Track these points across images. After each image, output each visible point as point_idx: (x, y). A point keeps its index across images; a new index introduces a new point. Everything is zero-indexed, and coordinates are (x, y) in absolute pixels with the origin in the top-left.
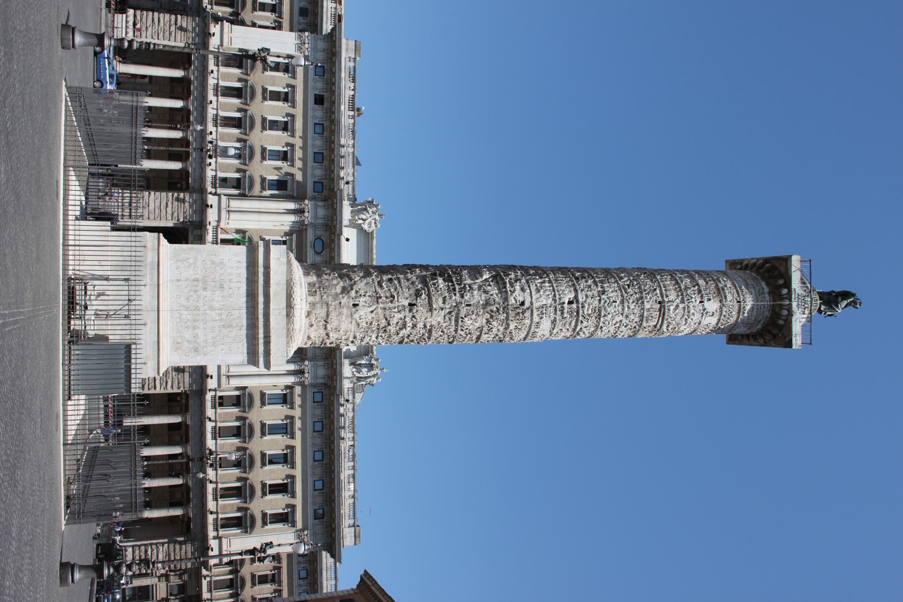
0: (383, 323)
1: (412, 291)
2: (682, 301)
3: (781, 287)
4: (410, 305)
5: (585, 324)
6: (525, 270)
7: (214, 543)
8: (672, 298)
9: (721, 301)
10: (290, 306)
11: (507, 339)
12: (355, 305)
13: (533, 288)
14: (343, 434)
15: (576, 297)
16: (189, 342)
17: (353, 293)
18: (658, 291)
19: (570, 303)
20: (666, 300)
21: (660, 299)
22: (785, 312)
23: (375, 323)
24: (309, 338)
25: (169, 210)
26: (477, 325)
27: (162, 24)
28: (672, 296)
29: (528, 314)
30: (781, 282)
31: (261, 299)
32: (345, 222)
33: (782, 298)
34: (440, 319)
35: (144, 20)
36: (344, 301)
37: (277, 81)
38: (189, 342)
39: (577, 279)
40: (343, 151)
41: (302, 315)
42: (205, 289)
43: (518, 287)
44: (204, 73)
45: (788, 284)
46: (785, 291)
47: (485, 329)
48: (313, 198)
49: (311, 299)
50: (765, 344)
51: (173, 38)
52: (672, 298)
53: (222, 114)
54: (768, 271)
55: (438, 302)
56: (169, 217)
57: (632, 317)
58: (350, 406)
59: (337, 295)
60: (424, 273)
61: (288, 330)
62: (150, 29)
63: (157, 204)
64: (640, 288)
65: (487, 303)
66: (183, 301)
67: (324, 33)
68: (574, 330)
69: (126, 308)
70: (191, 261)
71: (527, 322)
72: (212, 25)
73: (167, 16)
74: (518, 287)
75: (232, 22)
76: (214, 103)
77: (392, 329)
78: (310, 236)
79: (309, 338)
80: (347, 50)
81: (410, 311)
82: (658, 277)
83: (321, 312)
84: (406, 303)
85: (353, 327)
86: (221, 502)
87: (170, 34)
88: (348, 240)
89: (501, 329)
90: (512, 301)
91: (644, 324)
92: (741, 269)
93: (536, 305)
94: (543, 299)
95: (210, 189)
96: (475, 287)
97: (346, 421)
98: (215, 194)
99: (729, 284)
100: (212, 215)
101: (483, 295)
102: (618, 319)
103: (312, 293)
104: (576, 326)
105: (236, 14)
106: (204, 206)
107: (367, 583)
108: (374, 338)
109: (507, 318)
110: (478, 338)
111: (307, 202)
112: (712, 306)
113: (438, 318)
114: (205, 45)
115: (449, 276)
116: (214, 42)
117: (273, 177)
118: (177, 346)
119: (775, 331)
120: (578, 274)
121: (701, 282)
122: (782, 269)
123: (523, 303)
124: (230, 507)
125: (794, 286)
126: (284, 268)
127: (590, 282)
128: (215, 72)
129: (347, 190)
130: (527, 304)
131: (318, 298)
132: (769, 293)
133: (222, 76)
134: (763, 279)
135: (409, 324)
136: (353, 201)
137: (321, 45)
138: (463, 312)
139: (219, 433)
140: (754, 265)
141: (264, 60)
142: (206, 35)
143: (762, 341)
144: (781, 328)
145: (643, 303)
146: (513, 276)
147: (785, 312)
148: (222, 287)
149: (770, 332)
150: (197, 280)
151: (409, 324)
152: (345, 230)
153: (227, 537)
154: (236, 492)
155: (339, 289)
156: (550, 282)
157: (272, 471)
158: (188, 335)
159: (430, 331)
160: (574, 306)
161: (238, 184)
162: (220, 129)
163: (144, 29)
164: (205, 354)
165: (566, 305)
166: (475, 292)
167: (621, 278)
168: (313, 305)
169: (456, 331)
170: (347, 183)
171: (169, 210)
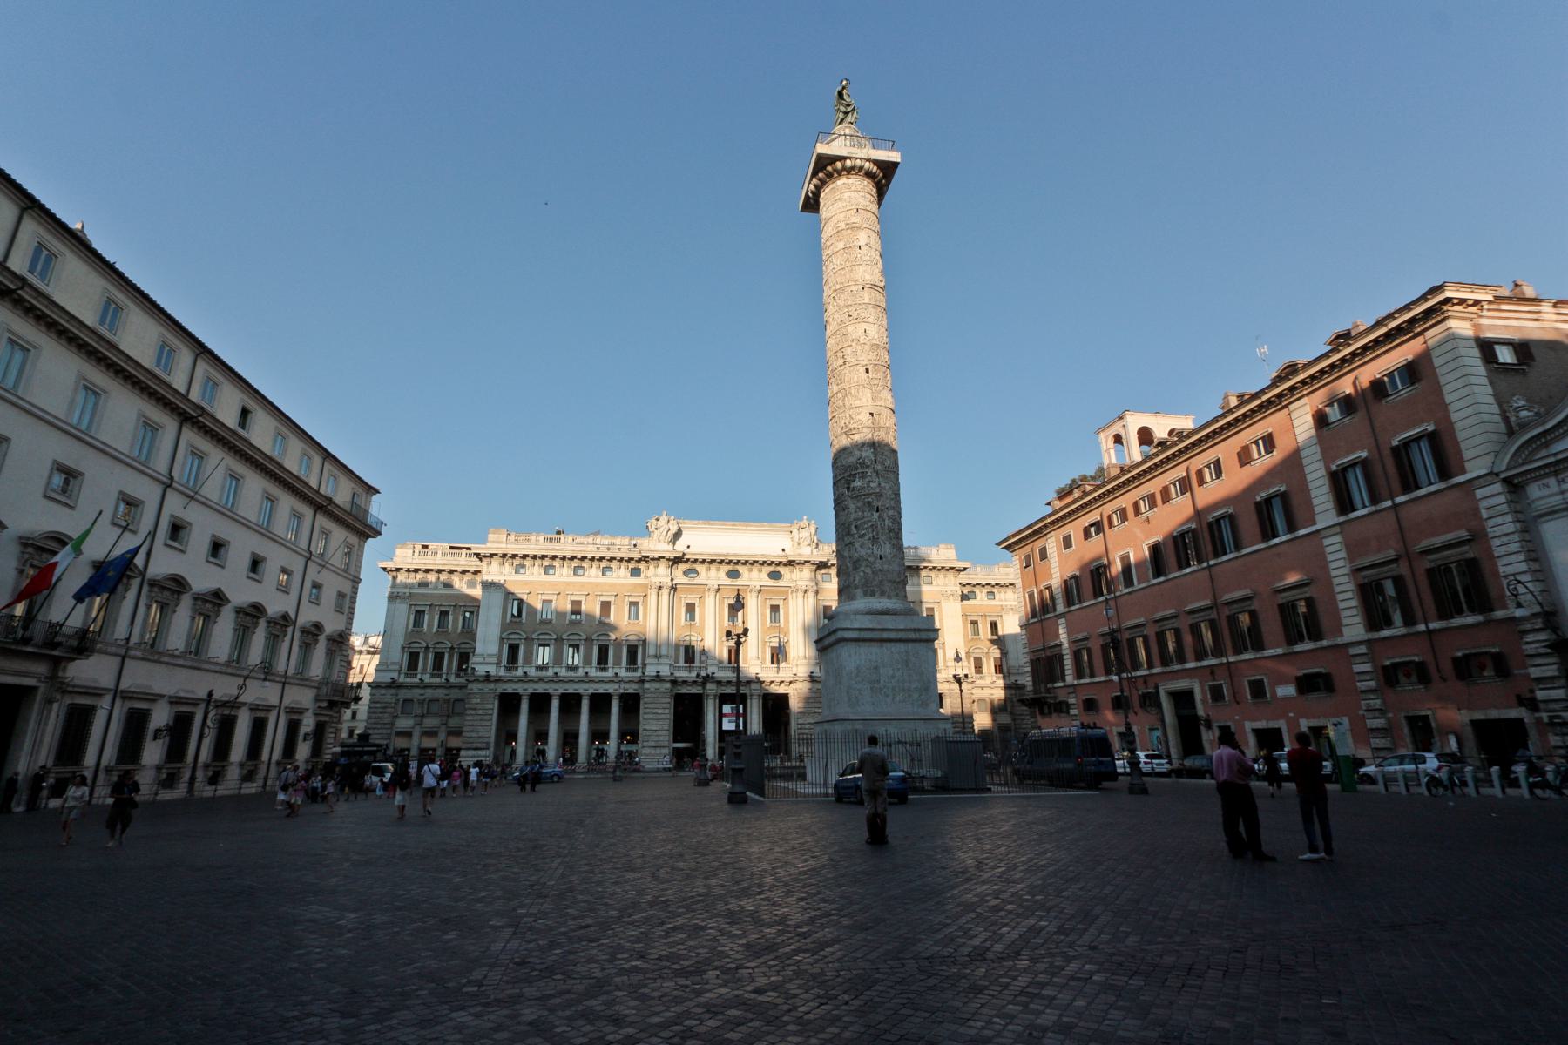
13: (857, 403)
31: (885, 635)
66: (889, 700)
84: (876, 515)
95: (639, 674)
100: (665, 671)
103: (873, 594)
106: (658, 678)
114: (499, 680)
116: (492, 670)
127: (849, 350)
142: (487, 678)
148: (876, 668)
155: (869, 571)
158: (915, 696)
168: (883, 593)
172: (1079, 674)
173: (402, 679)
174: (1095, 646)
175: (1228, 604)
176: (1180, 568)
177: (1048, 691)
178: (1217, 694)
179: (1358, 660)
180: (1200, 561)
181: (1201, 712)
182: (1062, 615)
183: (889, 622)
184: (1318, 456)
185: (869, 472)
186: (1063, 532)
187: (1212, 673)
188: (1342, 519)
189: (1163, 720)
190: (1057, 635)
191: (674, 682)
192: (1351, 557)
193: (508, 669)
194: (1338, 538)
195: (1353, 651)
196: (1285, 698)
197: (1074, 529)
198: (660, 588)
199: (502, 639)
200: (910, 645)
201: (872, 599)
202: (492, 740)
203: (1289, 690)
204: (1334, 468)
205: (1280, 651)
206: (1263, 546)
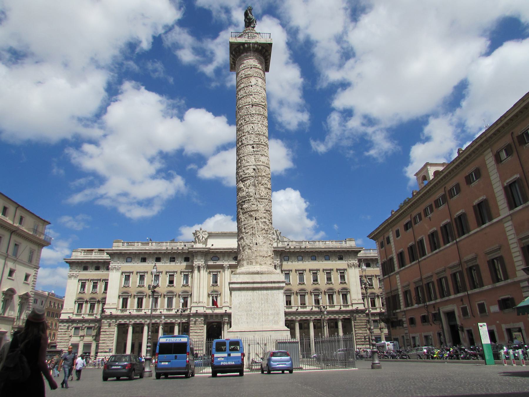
0: (264, 231)
1: (249, 218)
2: (252, 95)
3: (244, 47)
4: (256, 219)
5: (262, 141)
6: (238, 168)
7: (355, 307)
8: (250, 100)
9: (251, 77)
10: (258, 273)
11: (270, 176)
12: (256, 244)
13: (247, 164)
14: (303, 247)
15: (250, 145)
16: (274, 317)
17: (251, 245)
18: (247, 107)
19: (253, 147)
20: (251, 103)
21: (251, 106)
22: (256, 46)
23: (264, 235)
24: (271, 264)
25: (198, 331)
26: (264, 190)
27: (105, 339)
28: (249, 100)
29: (259, 167)
30: (242, 47)
31: (255, 285)
32: (204, 246)
33: (249, 47)
34: (262, 206)
35: (103, 347)
36: (255, 249)
37: (135, 280)
38: (274, 317)
39: (242, 144)
40: (169, 248)
41: (260, 266)
42: (251, 311)
43: (247, 171)
44: (130, 317)
45: (243, 44)
46: (246, 46)
47: (265, 186)
48: (193, 262)
49: (254, 264)
50: (270, 55)
51: (113, 333)
52: (250, 100)
53: (166, 307)
54: (236, 53)
55: (254, 207)
56: (202, 331)
57: (259, 119)
58: (290, 243)
59: (252, 252)
60: (241, 213)
61: (268, 274)
62: (108, 344)
63: (196, 337)
64: (246, 115)
65: (254, 185)
66: (256, 321)
67: (109, 258)
68: (265, 146)
69: (262, 345)
70: (239, 317)
71: (262, 167)
72: (106, 314)
73: (101, 336)
74: (247, 171)
75: (104, 304)
76: (146, 311)
77: (266, 227)
78: (211, 263)
79: (271, 264)
80: (118, 247)
81: (258, 219)
82: (240, 106)
83: (259, 259)
84: (255, 221)
85: (266, 245)
86: (335, 303)
87: (111, 334)
88: (212, 245)
89: (265, 179)
90: (253, 174)
91: (262, 113)
92: (235, 65)
93: (254, 163)
94: (252, 160)
96: (247, 190)
97: (297, 246)
98: (191, 309)
99: (243, 72)
100: (201, 310)
101: (251, 187)
102: (260, 126)
103: (251, 263)
104: (263, 145)
105: (99, 302)
106: (197, 315)
107: (374, 236)
108: (270, 236)
109: (261, 176)
110: (269, 189)
111: (194, 265)
112: (253, 81)
113: (261, 207)
114: (117, 317)
115: (242, 202)
116: (114, 312)
117: (183, 282)
118: (276, 322)
119: (264, 50)
120: (240, 144)
121: (242, 86)
122: (235, 46)
123: (254, 169)
124: (338, 299)
125: (244, 41)
126: (241, 276)
127: (244, 138)
128: (130, 311)
129: (188, 245)
130: (254, 167)
131: (253, 261)
132: (247, 53)
133: (132, 309)
134: (240, 55)
135: (264, 220)
136: (195, 242)
137: (116, 259)
138: (258, 196)
139: (303, 304)
140: (233, 59)
141: (155, 287)
142: (111, 317)
143: (268, 57)
144: (263, 48)
145: (253, 114)
146: (242, 173)
147: (256, 46)
148: (250, 303)
149: (264, 53)
150: (247, 315)
151: (264, 220)
152: (208, 247)
153: (351, 301)
154: (331, 297)
155: (249, 251)
156: (244, 156)
157: (321, 280)
158: (271, 318)
159: (267, 211)
160: (255, 146)
161: (185, 299)
162: (173, 308)
163: (108, 347)
164: (279, 310)
165: (254, 150)
166: (249, 190)
167: (241, 123)
168: (257, 263)
169: (267, 199)
170: (185, 245)
171: (198, 331)
172: (407, 305)
173: (74, 317)
174: (412, 288)
175: (466, 262)
176: (445, 244)
177: (394, 314)
178: (464, 311)
179: (525, 290)
180: (453, 240)
181: (458, 323)
182: (398, 273)
183: (257, 278)
184: (498, 179)
185: (252, 198)
186: (395, 229)
187: (462, 300)
188: (512, 212)
189: (442, 328)
190: (396, 284)
191: (205, 316)
192: (517, 234)
193: (122, 311)
194: (510, 223)
195: (522, 285)
196: (495, 313)
197: (400, 226)
198: (199, 268)
199: (119, 296)
200: (269, 292)
201: (250, 266)
202: (114, 347)
203: (495, 308)
204: (505, 184)
205: (490, 287)
206: (478, 229)
